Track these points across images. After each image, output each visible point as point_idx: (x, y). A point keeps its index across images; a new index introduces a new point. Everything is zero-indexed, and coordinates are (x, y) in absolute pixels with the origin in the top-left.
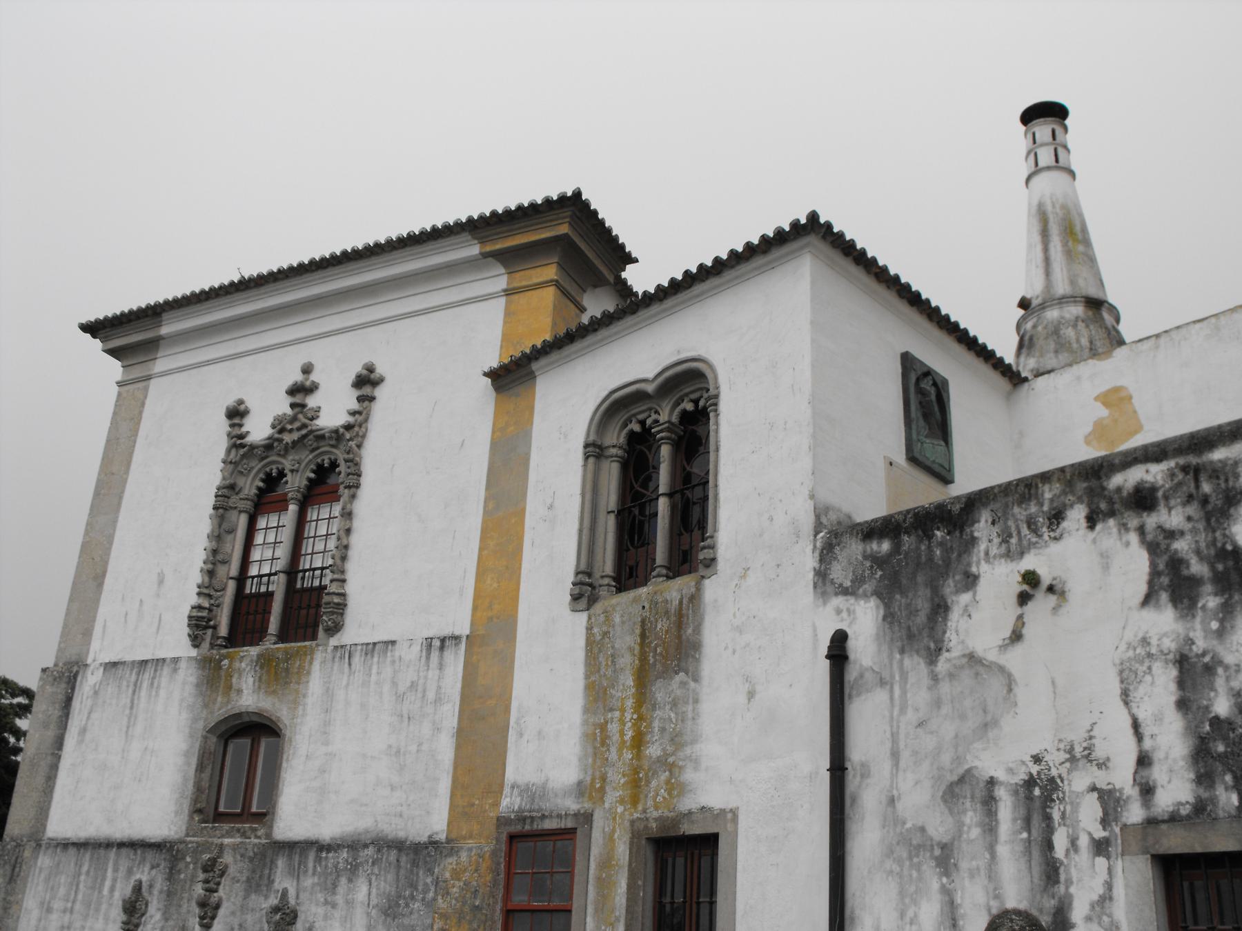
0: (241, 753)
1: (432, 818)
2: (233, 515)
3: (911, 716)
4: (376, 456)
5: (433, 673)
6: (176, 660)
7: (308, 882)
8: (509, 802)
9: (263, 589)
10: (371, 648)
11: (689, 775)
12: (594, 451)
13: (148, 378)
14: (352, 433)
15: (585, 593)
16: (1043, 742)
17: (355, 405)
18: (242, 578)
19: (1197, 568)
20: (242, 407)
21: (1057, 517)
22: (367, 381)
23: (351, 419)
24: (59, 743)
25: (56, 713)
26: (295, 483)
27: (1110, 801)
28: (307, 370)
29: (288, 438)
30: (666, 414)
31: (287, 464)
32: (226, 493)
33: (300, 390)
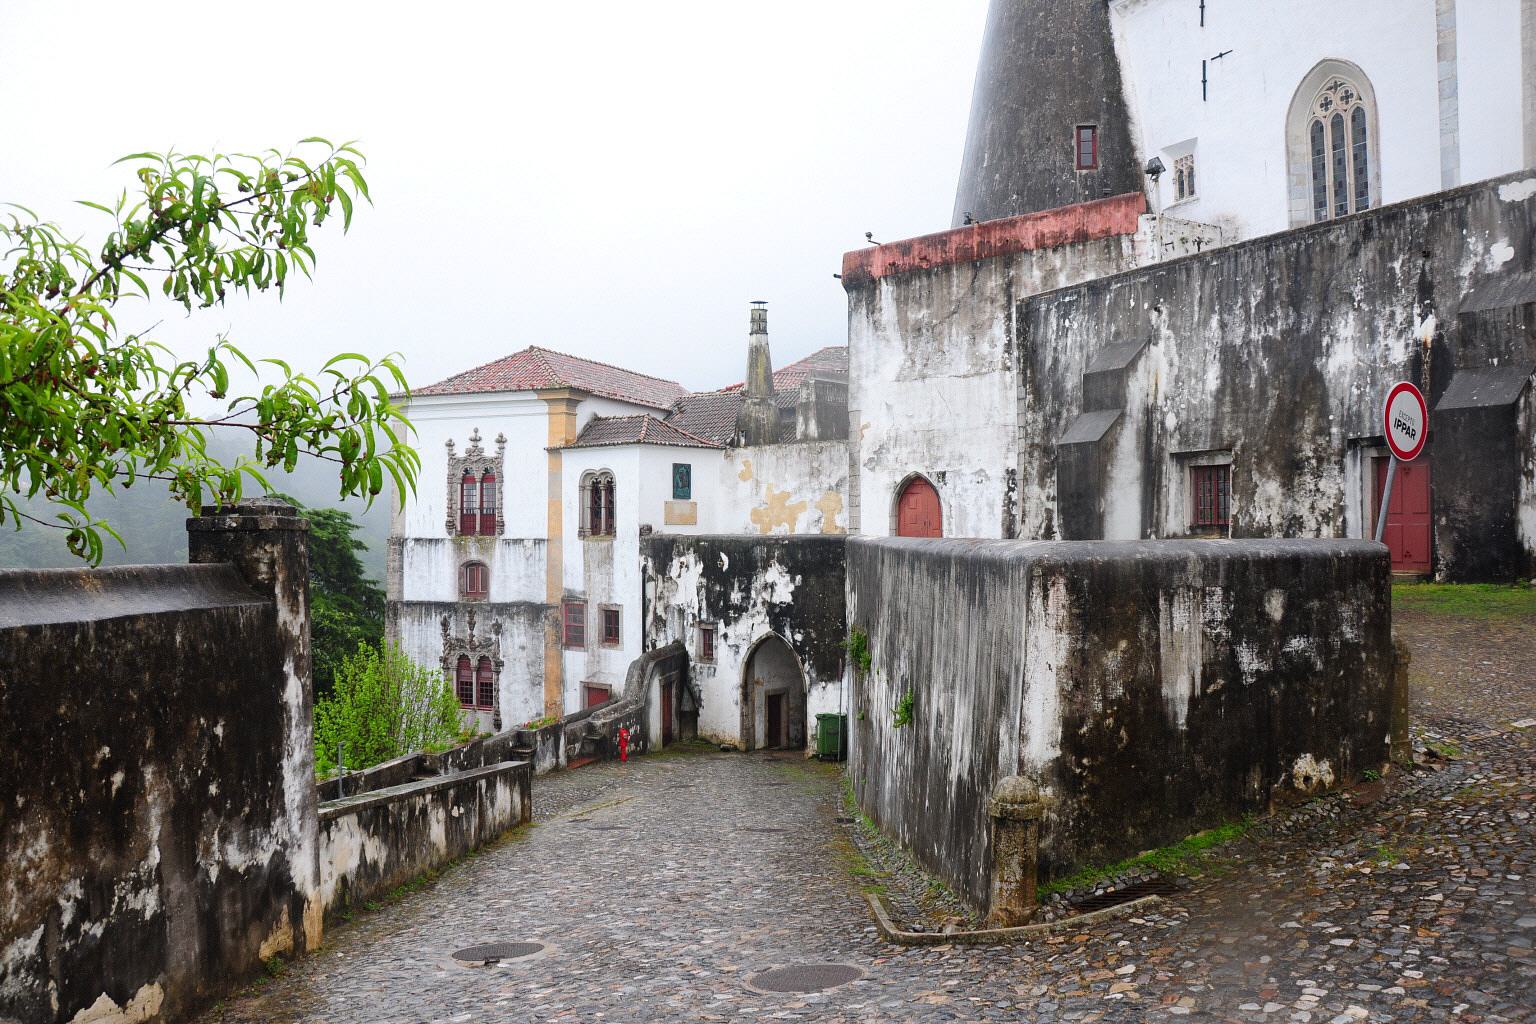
1: (540, 596)
4: (509, 470)
12: (582, 488)
14: (498, 460)
22: (501, 440)
26: (478, 476)
27: (694, 615)
28: (476, 431)
30: (603, 480)
32: (451, 477)
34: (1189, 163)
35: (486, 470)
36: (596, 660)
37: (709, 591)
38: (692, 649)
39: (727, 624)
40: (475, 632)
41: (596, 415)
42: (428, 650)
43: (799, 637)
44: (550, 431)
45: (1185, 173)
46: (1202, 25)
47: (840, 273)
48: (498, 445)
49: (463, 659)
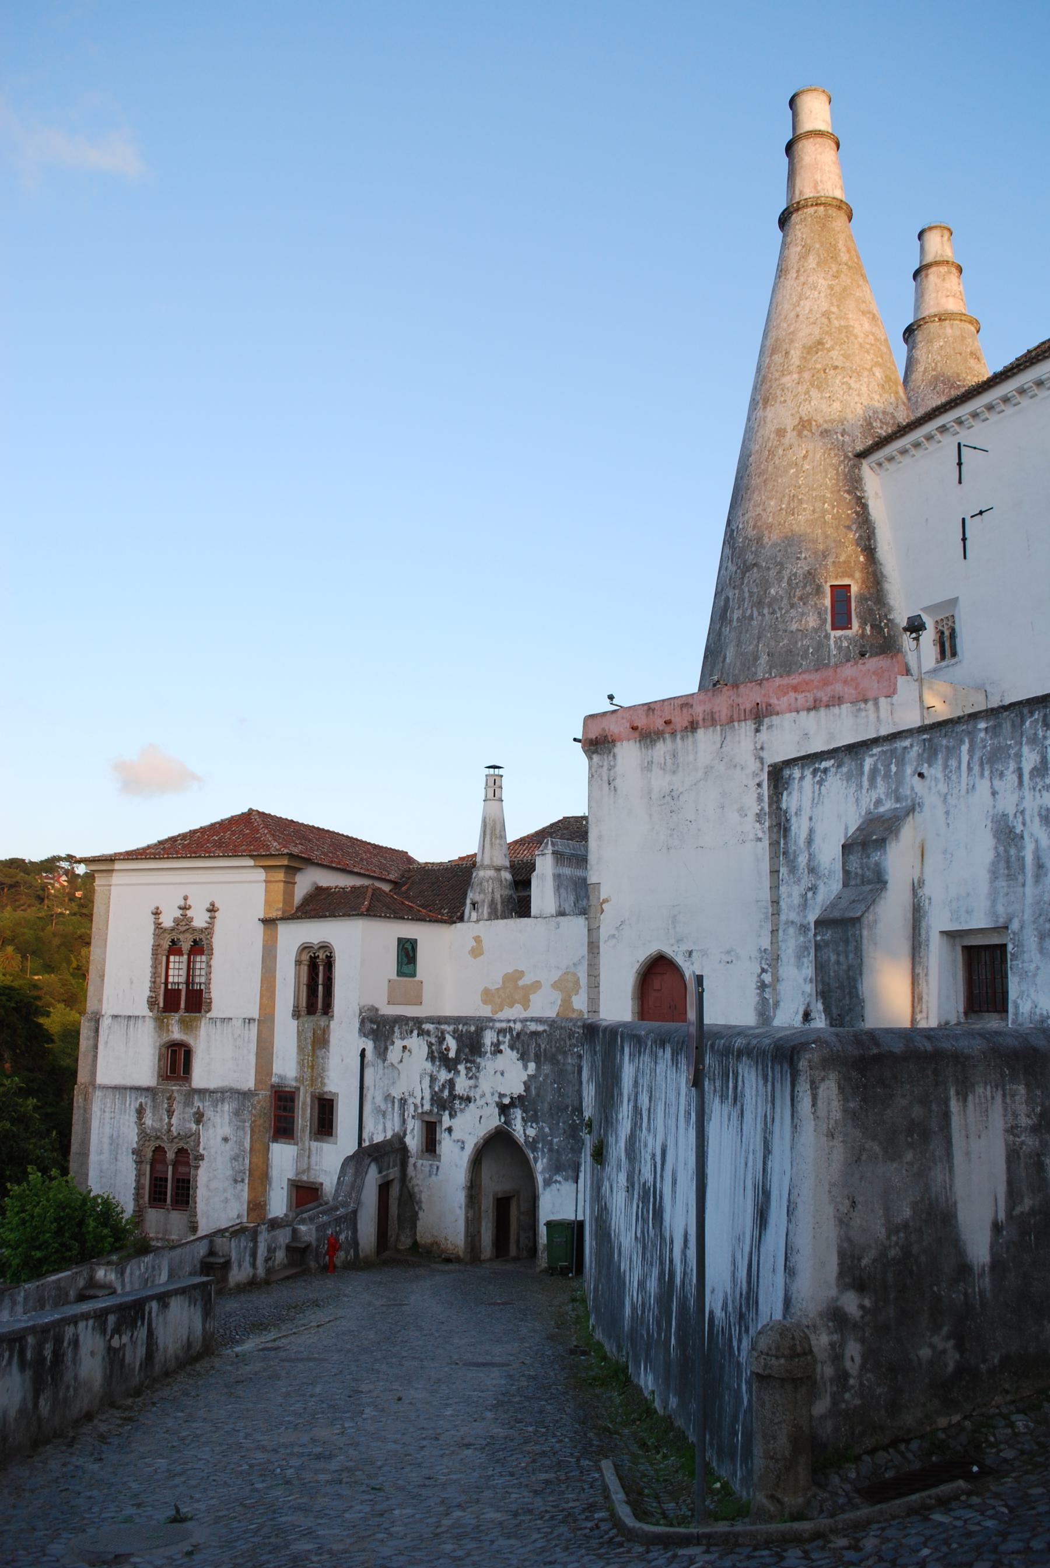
0: (177, 1061)
1: (249, 1083)
3: (379, 1076)
4: (218, 941)
5: (247, 1032)
6: (144, 1017)
7: (207, 1104)
8: (274, 1080)
10: (223, 1020)
11: (326, 1081)
12: (298, 963)
14: (209, 930)
15: (296, 1014)
16: (404, 1090)
18: (166, 983)
19: (436, 1054)
21: (411, 1032)
22: (212, 909)
24: (96, 1047)
25: (93, 1034)
26: (186, 946)
27: (415, 1105)
28: (186, 898)
30: (322, 955)
31: (181, 937)
34: (950, 623)
35: (195, 941)
36: (305, 1155)
37: (433, 1079)
38: (413, 1142)
39: (451, 1116)
40: (174, 1121)
41: (315, 883)
42: (121, 1142)
43: (532, 1132)
44: (266, 901)
45: (947, 633)
46: (960, 482)
47: (580, 737)
48: (209, 914)
49: (159, 1150)
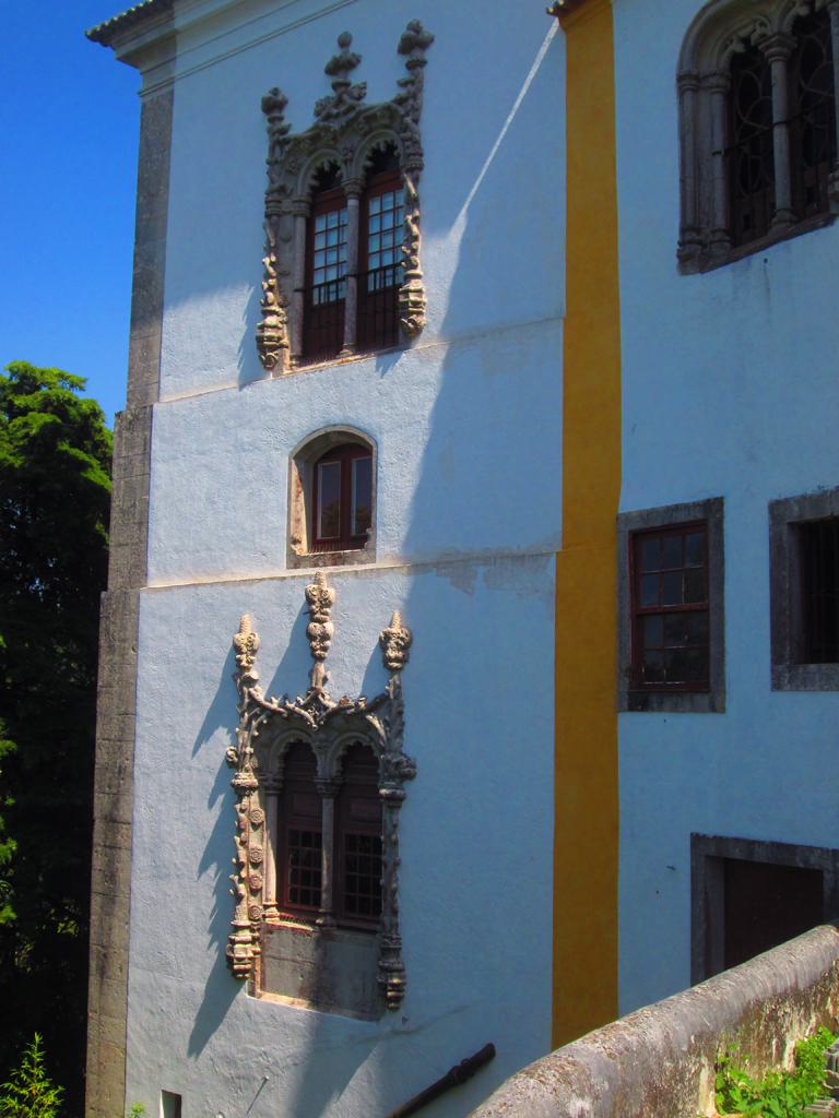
2: (288, 220)
4: (435, 130)
9: (333, 298)
12: (689, 83)
13: (171, 82)
14: (406, 107)
17: (404, 74)
20: (280, 98)
22: (414, 45)
23: (403, 92)
26: (352, 174)
28: (344, 42)
29: (335, 125)
33: (341, 67)
35: (377, 156)
